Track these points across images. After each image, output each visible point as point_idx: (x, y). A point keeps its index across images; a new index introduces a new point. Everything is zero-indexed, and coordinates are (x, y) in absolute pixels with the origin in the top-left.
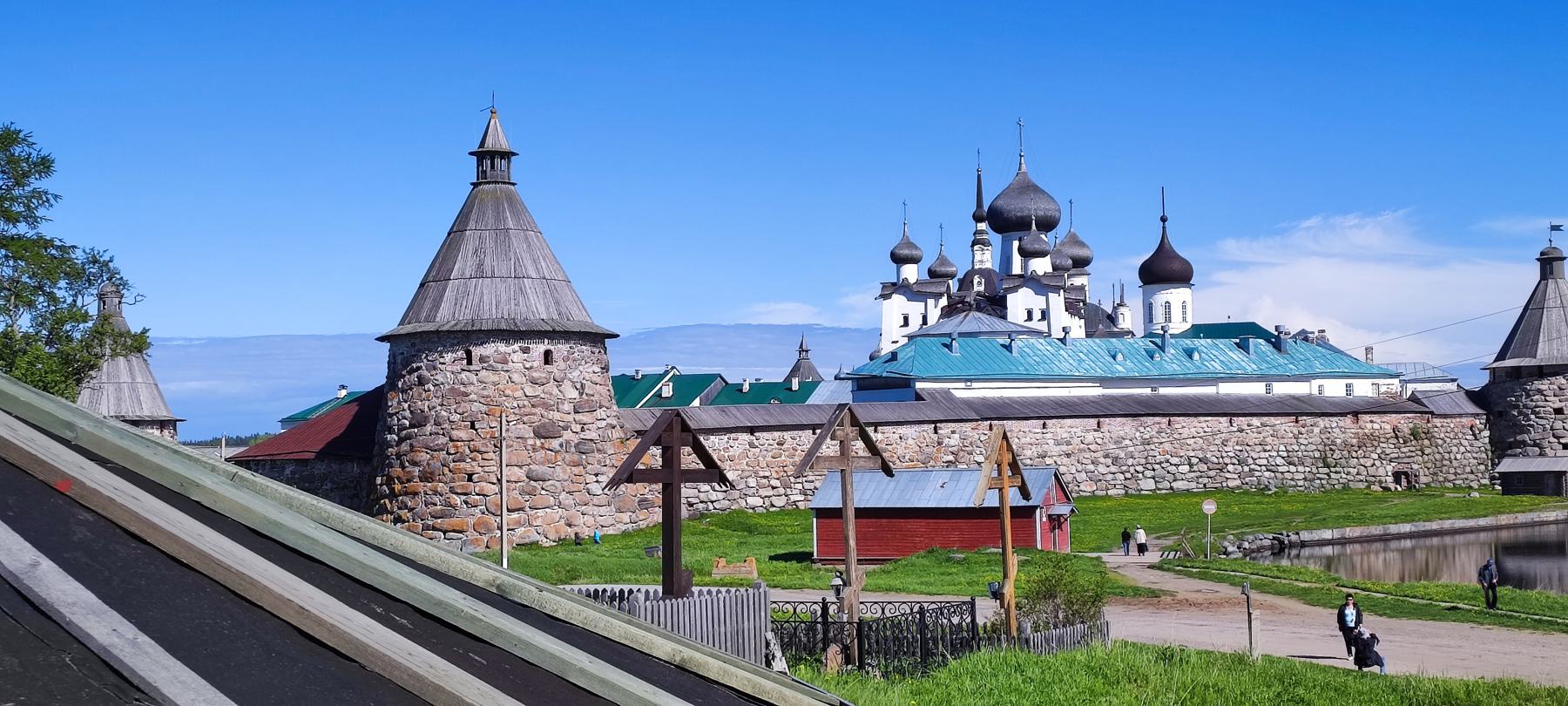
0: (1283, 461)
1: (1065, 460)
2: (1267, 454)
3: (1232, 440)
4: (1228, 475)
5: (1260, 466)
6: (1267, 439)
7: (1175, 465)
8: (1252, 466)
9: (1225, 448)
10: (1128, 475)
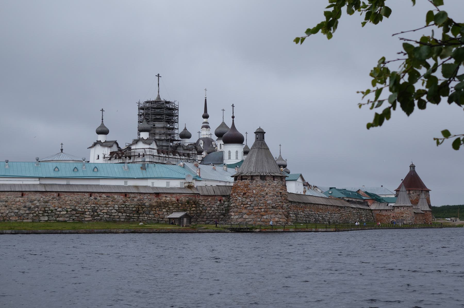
0: (116, 211)
1: (4, 208)
2: (108, 208)
3: (90, 203)
4: (86, 216)
5: (103, 213)
6: (110, 203)
7: (59, 211)
8: (99, 213)
9: (87, 206)
10: (35, 215)
